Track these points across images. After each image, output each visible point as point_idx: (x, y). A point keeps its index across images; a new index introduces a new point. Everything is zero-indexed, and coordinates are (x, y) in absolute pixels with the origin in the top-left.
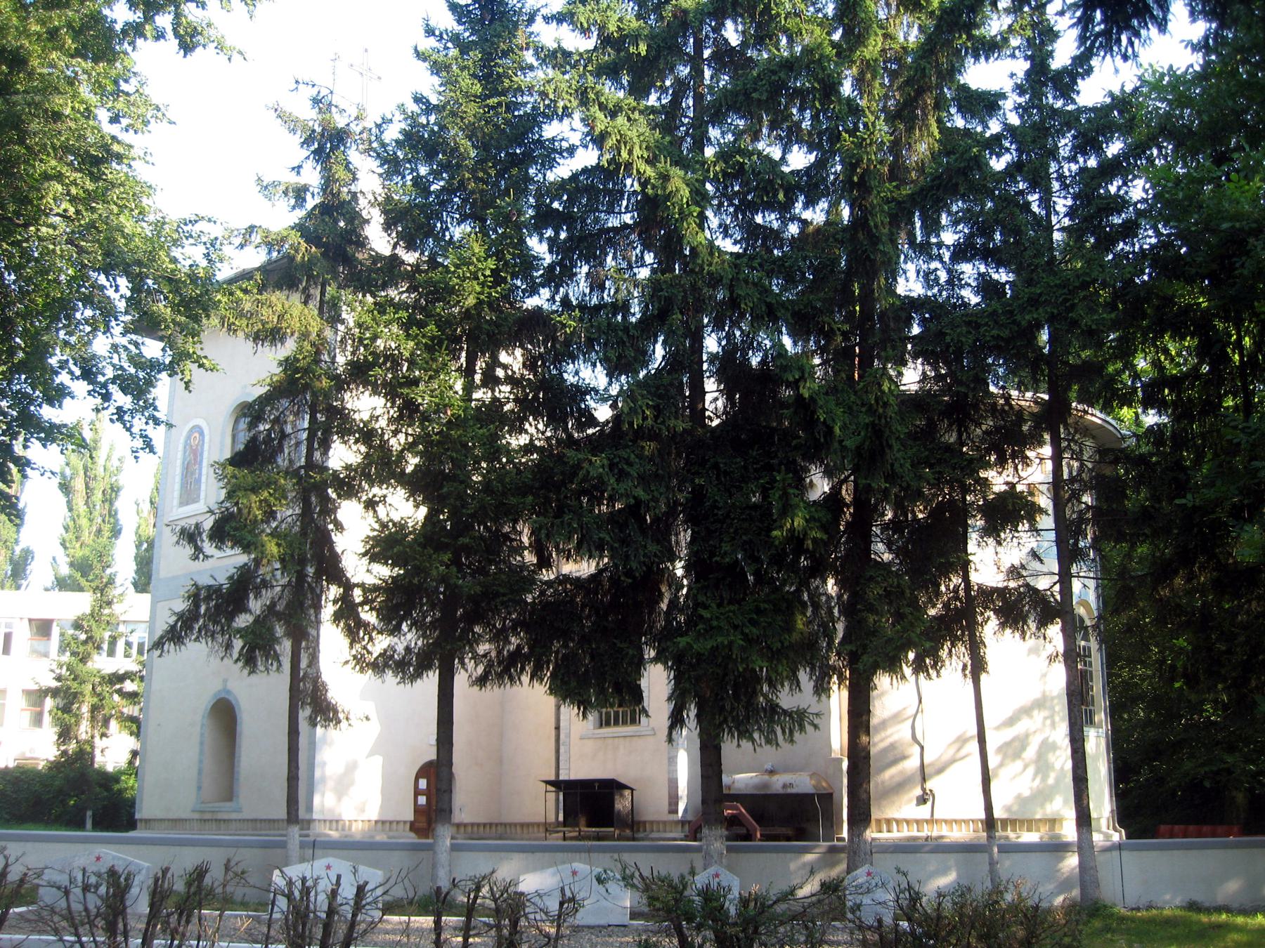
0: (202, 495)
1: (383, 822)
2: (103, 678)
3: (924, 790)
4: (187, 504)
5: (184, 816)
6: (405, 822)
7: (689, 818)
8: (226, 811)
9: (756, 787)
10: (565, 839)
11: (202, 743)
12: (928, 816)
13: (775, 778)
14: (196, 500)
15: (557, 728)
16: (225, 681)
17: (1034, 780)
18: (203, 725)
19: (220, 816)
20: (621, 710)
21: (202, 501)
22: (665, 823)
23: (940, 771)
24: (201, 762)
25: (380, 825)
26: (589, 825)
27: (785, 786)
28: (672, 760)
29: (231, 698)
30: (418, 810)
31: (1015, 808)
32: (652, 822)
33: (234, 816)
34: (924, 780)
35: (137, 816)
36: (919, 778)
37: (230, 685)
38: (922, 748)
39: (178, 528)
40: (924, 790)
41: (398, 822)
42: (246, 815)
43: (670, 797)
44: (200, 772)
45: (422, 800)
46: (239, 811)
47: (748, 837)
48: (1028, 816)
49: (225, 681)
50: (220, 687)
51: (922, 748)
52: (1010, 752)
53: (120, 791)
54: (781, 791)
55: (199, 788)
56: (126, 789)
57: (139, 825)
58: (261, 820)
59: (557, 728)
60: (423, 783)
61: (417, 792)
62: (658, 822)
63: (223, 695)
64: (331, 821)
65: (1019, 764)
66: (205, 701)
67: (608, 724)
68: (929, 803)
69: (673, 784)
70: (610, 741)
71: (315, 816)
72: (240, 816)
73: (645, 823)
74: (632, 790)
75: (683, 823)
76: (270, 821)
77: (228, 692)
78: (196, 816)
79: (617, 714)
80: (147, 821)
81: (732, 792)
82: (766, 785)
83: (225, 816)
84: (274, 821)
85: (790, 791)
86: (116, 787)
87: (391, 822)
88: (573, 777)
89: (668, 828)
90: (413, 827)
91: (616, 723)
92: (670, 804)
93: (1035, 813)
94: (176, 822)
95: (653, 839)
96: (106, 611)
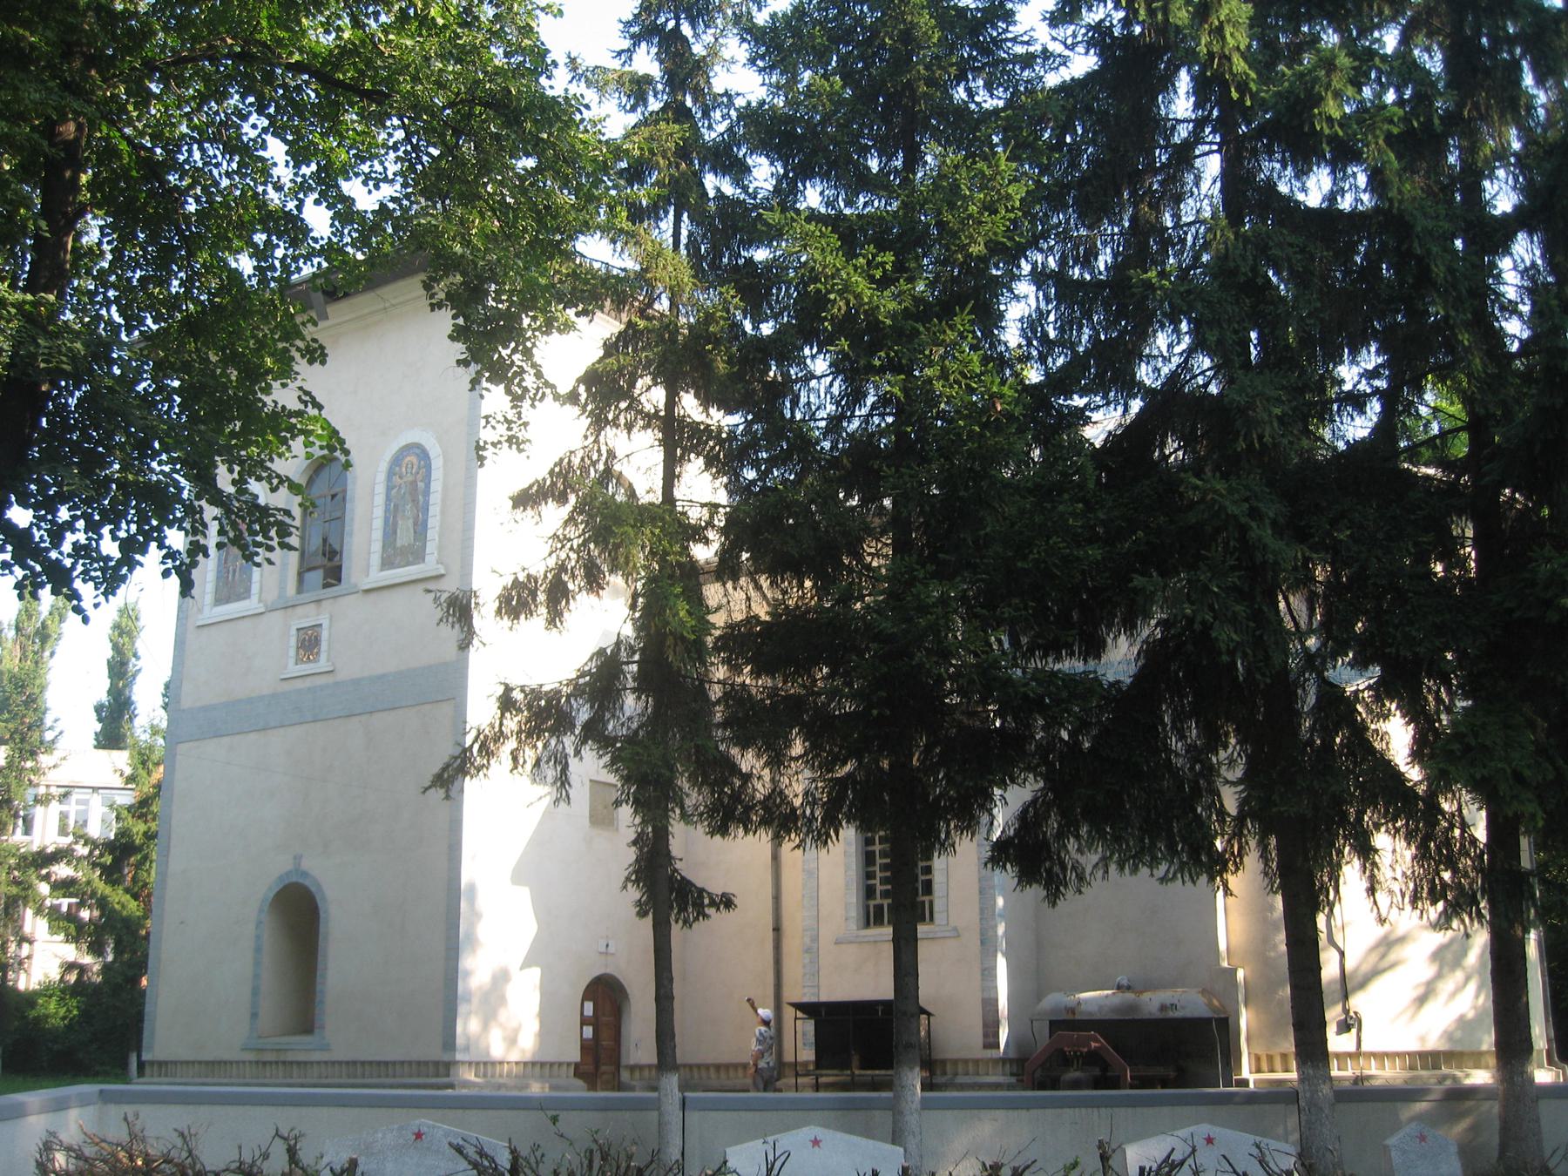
0: (255, 588)
1: (543, 1064)
2: (24, 858)
3: (1346, 1011)
4: (228, 601)
5: (226, 1057)
6: (569, 1064)
7: (1012, 1055)
8: (300, 1048)
9: (1116, 1010)
10: (817, 1088)
11: (258, 950)
12: (1352, 1048)
13: (1146, 996)
14: (246, 594)
15: (777, 929)
16: (298, 858)
17: (1477, 997)
18: (259, 923)
19: (290, 1057)
21: (255, 598)
22: (977, 1062)
23: (1362, 985)
24: (256, 976)
25: (538, 1068)
26: (862, 1068)
27: (1163, 1008)
28: (989, 973)
29: (307, 883)
30: (586, 1047)
31: (1458, 1034)
32: (955, 1062)
33: (316, 1056)
34: (1346, 997)
36: (1338, 995)
37: (306, 865)
38: (1342, 954)
39: (445, 596)
40: (1346, 1011)
41: (560, 1064)
42: (339, 1054)
43: (985, 1025)
44: (255, 992)
45: (588, 1032)
46: (326, 1048)
47: (1114, 1083)
48: (1466, 1048)
49: (298, 858)
50: (289, 867)
51: (1342, 954)
52: (1449, 956)
53: (37, 1020)
54: (1159, 1015)
55: (254, 1015)
56: (47, 1016)
58: (363, 1063)
59: (777, 929)
60: (589, 1008)
61: (584, 1021)
62: (966, 1061)
63: (294, 879)
64: (478, 1063)
65: (1459, 975)
66: (264, 886)
68: (1354, 1031)
69: (990, 1004)
71: (459, 1057)
72: (325, 1056)
73: (944, 1062)
74: (929, 1014)
75: (1004, 1061)
76: (379, 1063)
77: (305, 874)
80: (162, 1065)
81: (1078, 1017)
82: (1133, 1007)
83: (301, 1057)
84: (386, 1063)
85: (1171, 1014)
86: (33, 1014)
87: (552, 1064)
88: (824, 998)
90: (579, 1071)
92: (985, 1035)
93: (1480, 1042)
94: (214, 1067)
95: (962, 1087)
96: (29, 764)
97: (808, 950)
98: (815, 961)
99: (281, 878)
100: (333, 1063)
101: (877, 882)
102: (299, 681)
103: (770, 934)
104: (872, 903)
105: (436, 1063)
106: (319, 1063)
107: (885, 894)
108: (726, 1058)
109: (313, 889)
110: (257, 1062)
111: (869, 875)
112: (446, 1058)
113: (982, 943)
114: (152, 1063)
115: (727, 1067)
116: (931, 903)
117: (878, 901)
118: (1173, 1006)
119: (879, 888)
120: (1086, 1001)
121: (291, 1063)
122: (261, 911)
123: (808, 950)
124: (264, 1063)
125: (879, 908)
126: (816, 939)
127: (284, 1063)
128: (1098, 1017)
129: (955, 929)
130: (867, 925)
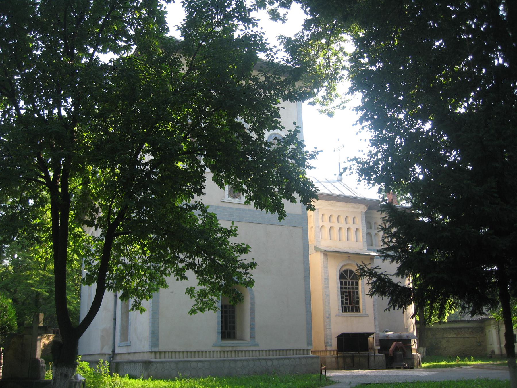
19: (239, 349)
27: (407, 337)
46: (257, 345)
54: (407, 338)
67: (345, 311)
70: (349, 318)
72: (257, 348)
78: (218, 349)
82: (400, 336)
83: (245, 349)
91: (349, 311)
97: (328, 318)
100: (259, 351)
102: (231, 204)
104: (343, 305)
105: (304, 350)
106: (253, 351)
107: (347, 303)
110: (221, 351)
111: (342, 298)
112: (309, 348)
117: (345, 305)
121: (238, 351)
123: (328, 318)
124: (224, 352)
126: (330, 315)
127: (235, 351)
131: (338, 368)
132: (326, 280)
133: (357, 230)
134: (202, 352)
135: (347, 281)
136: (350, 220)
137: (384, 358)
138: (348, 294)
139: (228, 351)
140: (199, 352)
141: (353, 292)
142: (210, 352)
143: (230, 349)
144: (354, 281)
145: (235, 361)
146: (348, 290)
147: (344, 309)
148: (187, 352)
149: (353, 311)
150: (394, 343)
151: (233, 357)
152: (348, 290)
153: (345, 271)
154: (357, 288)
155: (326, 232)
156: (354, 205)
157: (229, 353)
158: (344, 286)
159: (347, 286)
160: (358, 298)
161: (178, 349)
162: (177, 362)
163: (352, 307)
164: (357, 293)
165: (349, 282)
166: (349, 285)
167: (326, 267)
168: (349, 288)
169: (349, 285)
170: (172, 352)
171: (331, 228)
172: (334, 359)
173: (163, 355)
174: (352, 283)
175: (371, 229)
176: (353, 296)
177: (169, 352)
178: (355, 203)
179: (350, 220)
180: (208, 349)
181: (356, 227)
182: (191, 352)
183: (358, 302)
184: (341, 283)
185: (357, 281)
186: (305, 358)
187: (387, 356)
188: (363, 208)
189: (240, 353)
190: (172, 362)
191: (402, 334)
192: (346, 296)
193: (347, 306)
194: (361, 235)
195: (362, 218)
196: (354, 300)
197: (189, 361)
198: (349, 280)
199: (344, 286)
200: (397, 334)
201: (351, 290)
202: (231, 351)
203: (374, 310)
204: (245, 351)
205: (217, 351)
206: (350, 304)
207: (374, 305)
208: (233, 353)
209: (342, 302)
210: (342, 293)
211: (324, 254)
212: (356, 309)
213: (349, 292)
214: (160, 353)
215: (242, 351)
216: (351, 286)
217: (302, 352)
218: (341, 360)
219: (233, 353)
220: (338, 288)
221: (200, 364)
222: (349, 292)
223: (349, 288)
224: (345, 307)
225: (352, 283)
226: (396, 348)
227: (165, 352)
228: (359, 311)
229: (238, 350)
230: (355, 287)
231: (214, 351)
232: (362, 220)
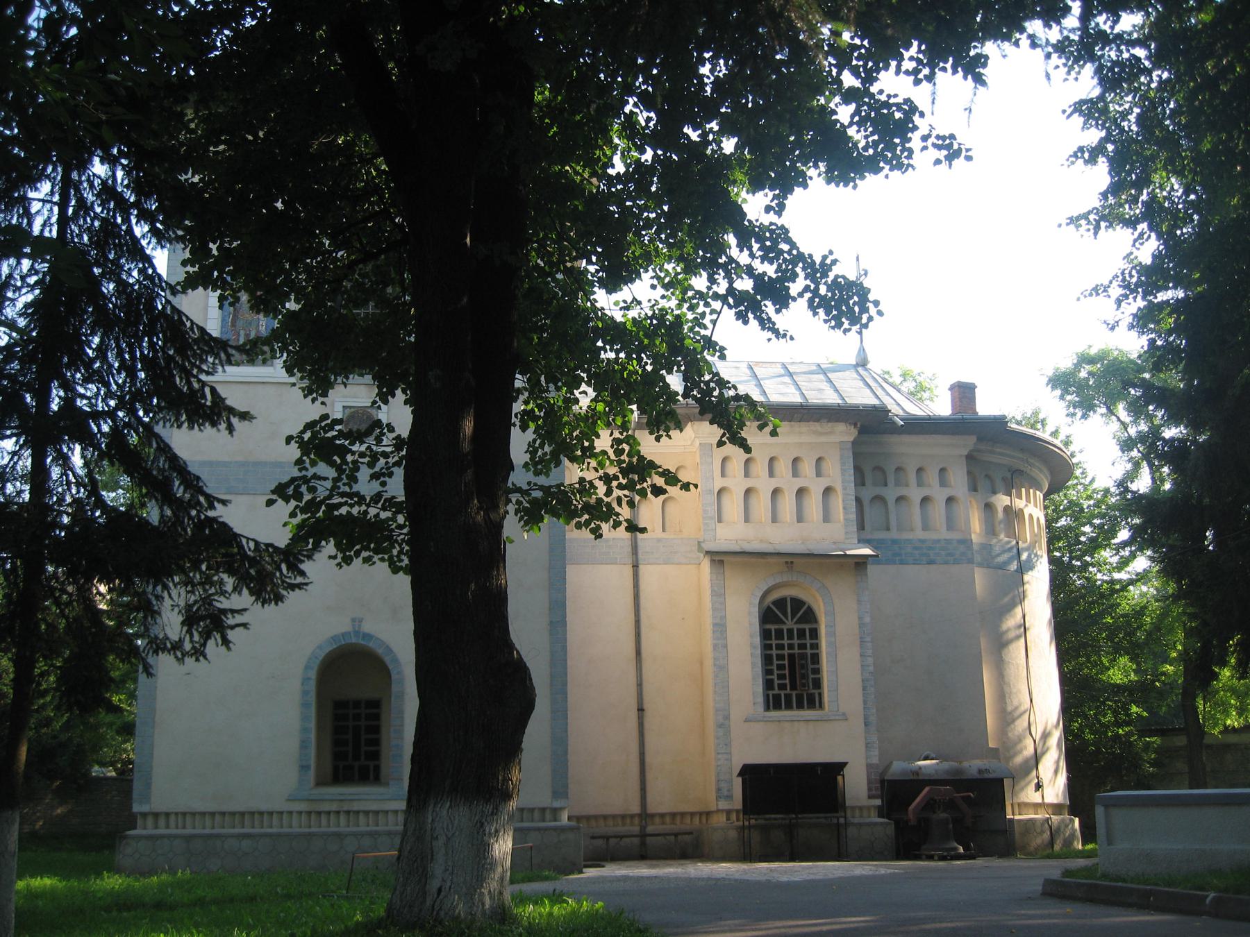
12: (1040, 801)
15: (641, 710)
18: (305, 680)
19: (356, 806)
20: (794, 693)
22: (861, 808)
27: (980, 771)
29: (371, 645)
35: (136, 808)
37: (367, 627)
54: (979, 776)
57: (140, 822)
59: (641, 710)
63: (354, 640)
67: (777, 706)
70: (787, 725)
77: (368, 636)
78: (303, 807)
79: (788, 697)
82: (959, 771)
83: (374, 807)
85: (986, 776)
89: (865, 813)
91: (789, 706)
98: (728, 733)
99: (334, 638)
101: (775, 677)
103: (633, 714)
104: (771, 693)
105: (543, 810)
108: (592, 812)
109: (380, 651)
110: (309, 813)
111: (768, 672)
112: (557, 804)
113: (866, 724)
114: (144, 815)
115: (588, 818)
116: (820, 694)
117: (776, 691)
118: (987, 771)
119: (776, 682)
120: (925, 767)
121: (358, 812)
122: (307, 668)
123: (720, 726)
124: (319, 813)
125: (777, 699)
126: (727, 718)
127: (348, 812)
128: (935, 777)
129: (844, 714)
130: (767, 708)
131: (747, 856)
132: (720, 628)
133: (828, 491)
134: (261, 813)
135: (785, 628)
136: (808, 468)
137: (891, 830)
138: (786, 662)
139: (329, 813)
140: (252, 813)
141: (803, 656)
142: (281, 813)
143: (334, 807)
144: (807, 627)
145: (339, 836)
146: (786, 652)
147: (773, 702)
148: (223, 814)
149: (800, 706)
150: (927, 789)
151: (343, 825)
152: (786, 652)
153: (780, 603)
154: (816, 646)
155: (733, 506)
156: (816, 426)
157: (332, 816)
158: (774, 642)
159: (786, 642)
160: (817, 671)
161: (199, 806)
162: (188, 839)
163: (799, 698)
164: (816, 658)
165: (790, 631)
166: (790, 637)
167: (719, 595)
168: (791, 647)
169: (790, 637)
170: (184, 814)
171: (748, 492)
172: (733, 834)
173: (162, 822)
174: (802, 634)
175: (886, 485)
176: (802, 667)
177: (176, 814)
178: (818, 420)
179: (808, 468)
180: (277, 807)
181: (824, 483)
182: (233, 814)
183: (818, 684)
184: (765, 634)
185: (814, 626)
186: (539, 829)
187: (901, 827)
188: (844, 433)
189: (361, 816)
190: (176, 837)
191: (965, 764)
192: (780, 667)
193: (782, 693)
194: (841, 506)
195: (842, 457)
196: (804, 676)
197: (218, 836)
198: (790, 624)
199: (774, 642)
200: (946, 765)
201: (796, 651)
202: (338, 812)
203: (865, 702)
204: (377, 813)
205: (300, 813)
206: (793, 687)
207: (864, 689)
208: (343, 818)
209: (768, 685)
210: (767, 659)
211: (712, 561)
212: (814, 702)
213: (791, 656)
214: (156, 815)
215: (367, 813)
216: (796, 641)
217: (537, 815)
218: (756, 837)
219: (343, 818)
220: (753, 646)
221: (246, 844)
222: (791, 656)
223: (791, 647)
224: (777, 699)
225: (802, 634)
226: (930, 805)
227: (167, 815)
228: (821, 706)
229: (356, 808)
230: (808, 642)
231: (291, 813)
232: (843, 464)
